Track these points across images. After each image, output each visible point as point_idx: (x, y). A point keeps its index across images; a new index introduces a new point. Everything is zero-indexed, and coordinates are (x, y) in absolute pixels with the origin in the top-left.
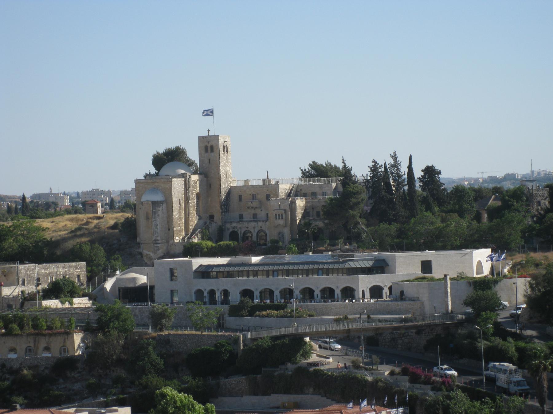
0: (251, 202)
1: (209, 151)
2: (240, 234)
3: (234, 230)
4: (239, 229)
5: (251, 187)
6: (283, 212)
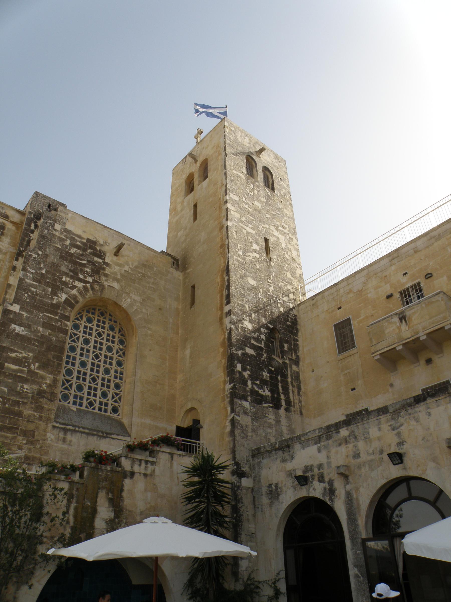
0: (396, 319)
1: (196, 183)
2: (352, 519)
3: (303, 493)
4: (338, 484)
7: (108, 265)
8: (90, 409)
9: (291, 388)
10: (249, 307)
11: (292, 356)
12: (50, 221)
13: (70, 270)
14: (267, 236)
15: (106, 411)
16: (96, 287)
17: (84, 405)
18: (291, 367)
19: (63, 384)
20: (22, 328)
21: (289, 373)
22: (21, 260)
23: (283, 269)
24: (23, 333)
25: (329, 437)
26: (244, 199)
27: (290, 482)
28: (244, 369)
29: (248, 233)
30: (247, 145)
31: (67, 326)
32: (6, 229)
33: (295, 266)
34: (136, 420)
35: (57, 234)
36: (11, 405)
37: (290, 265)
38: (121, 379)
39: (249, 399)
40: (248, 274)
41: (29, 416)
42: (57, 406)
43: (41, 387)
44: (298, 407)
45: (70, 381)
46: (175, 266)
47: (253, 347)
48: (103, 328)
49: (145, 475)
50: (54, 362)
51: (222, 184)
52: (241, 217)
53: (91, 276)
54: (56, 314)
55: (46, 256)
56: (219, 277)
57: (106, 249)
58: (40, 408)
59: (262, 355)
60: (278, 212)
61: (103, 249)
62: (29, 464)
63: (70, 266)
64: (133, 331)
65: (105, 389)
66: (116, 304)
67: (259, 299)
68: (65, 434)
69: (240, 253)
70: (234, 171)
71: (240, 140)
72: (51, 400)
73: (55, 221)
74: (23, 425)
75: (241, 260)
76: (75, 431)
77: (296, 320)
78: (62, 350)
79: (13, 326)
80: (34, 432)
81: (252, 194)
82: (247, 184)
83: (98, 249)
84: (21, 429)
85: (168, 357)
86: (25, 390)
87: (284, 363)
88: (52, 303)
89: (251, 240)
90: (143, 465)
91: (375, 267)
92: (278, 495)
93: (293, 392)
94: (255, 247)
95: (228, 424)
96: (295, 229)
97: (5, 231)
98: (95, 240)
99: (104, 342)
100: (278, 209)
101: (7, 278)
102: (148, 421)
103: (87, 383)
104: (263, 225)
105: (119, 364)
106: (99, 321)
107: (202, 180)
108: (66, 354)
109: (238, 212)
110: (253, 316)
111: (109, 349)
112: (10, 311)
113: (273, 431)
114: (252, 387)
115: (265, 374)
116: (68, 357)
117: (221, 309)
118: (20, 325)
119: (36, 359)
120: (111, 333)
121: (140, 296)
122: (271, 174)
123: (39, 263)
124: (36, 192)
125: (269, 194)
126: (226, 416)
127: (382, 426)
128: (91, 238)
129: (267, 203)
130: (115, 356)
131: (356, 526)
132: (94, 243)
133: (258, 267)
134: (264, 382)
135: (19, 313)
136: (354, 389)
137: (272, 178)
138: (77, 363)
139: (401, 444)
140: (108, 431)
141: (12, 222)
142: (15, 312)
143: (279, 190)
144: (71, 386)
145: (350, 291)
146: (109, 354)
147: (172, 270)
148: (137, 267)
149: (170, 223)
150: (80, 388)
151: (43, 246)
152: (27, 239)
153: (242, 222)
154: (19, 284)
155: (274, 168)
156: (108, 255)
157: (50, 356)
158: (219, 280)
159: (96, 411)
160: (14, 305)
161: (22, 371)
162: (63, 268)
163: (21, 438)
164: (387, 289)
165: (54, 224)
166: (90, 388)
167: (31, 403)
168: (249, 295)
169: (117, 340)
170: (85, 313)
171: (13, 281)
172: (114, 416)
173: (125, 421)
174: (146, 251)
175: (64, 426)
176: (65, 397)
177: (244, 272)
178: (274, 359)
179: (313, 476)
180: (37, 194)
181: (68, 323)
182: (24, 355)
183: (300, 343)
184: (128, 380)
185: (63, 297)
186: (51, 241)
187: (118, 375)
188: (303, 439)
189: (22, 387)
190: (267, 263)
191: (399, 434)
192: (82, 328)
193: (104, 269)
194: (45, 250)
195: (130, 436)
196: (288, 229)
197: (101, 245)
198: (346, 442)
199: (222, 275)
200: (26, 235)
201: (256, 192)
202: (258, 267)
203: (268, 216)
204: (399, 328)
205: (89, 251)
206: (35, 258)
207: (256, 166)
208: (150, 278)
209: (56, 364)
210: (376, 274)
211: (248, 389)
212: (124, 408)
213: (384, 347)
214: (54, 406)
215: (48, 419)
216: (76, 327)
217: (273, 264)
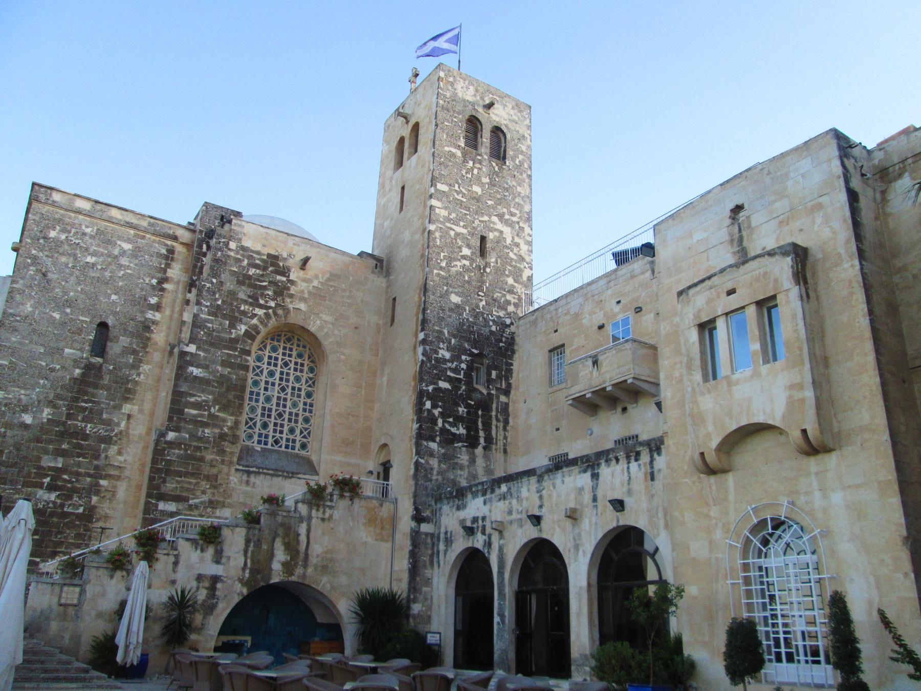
0: (590, 362)
5: (602, 283)
6: (784, 267)
7: (293, 282)
8: (276, 448)
9: (494, 422)
10: (448, 332)
11: (501, 385)
12: (223, 240)
13: (249, 297)
14: (485, 232)
15: (293, 448)
16: (280, 312)
17: (270, 444)
18: (498, 398)
19: (247, 423)
20: (200, 370)
21: (494, 406)
22: (194, 291)
23: (503, 274)
24: (201, 375)
25: (493, 491)
26: (456, 188)
27: (461, 531)
28: (434, 406)
29: (457, 234)
30: (470, 99)
31: (247, 361)
32: (176, 253)
33: (522, 266)
34: (325, 457)
35: (232, 254)
36: (193, 451)
37: (515, 267)
38: (311, 412)
39: (438, 439)
40: (451, 289)
41: (212, 461)
42: (239, 447)
43: (222, 429)
44: (502, 444)
45: (254, 419)
46: (378, 269)
47: (449, 380)
48: (290, 356)
49: (323, 520)
50: (235, 402)
51: (429, 168)
52: (450, 214)
53: (273, 300)
54: (235, 349)
55: (222, 283)
56: (417, 296)
57: (291, 262)
58: (221, 452)
59: (460, 388)
60: (507, 194)
61: (286, 264)
62: (213, 508)
63: (249, 291)
64: (323, 357)
65: (293, 424)
66: (303, 328)
67: (463, 320)
68: (248, 476)
69: (443, 264)
70: (447, 149)
71: (460, 95)
72: (233, 443)
73: (231, 238)
74: (206, 470)
75: (442, 273)
76: (259, 473)
77: (513, 339)
78: (243, 389)
79: (191, 369)
80: (217, 476)
81: (469, 176)
82: (464, 162)
83: (281, 264)
84: (204, 475)
85: (364, 384)
86: (206, 435)
87: (489, 394)
88: (230, 338)
89: (460, 243)
90: (321, 510)
91: (593, 287)
92: (452, 542)
93: (497, 427)
94: (466, 251)
95: (412, 467)
96: (530, 213)
97: (175, 256)
98: (277, 254)
99: (292, 371)
100: (507, 190)
101: (181, 315)
102: (339, 458)
103: (273, 420)
104: (481, 219)
105: (309, 395)
106: (285, 348)
107: (413, 151)
108: (248, 390)
109: (446, 208)
110: (453, 341)
111: (298, 379)
112: (186, 352)
113: (465, 473)
114: (443, 425)
115: (462, 410)
116: (252, 393)
117: (416, 336)
118: (198, 367)
119: (216, 401)
120: (299, 361)
121: (331, 315)
122: (504, 135)
123: (214, 294)
124: (206, 203)
125: (496, 169)
126: (412, 458)
127: (530, 487)
128: (273, 252)
129: (492, 184)
130: (304, 387)
131: (503, 579)
132: (276, 258)
133: (466, 278)
134: (459, 419)
135: (196, 354)
136: (558, 429)
137: (505, 143)
138: (262, 398)
139: (541, 507)
140: (295, 471)
141: (182, 243)
142: (192, 354)
143: (513, 159)
144: (255, 424)
145: (568, 313)
146: (297, 385)
147: (372, 277)
148: (329, 280)
149: (378, 204)
150: (265, 426)
151: (217, 273)
152: (199, 264)
153: (449, 220)
154: (194, 322)
155: (510, 126)
156: (293, 270)
157: (231, 397)
158: (416, 299)
159: (283, 449)
160: (190, 345)
161: (202, 416)
162: (242, 296)
163: (204, 483)
164: (599, 318)
165: (228, 243)
166: (275, 424)
167: (213, 447)
168: (450, 317)
169: (306, 368)
170: (269, 341)
171: (187, 317)
172: (303, 453)
173: (314, 458)
174: (339, 257)
175: (247, 469)
176: (250, 437)
177: (445, 288)
178: (478, 390)
179: (478, 527)
180: (206, 204)
181: (249, 358)
182: (203, 398)
183: (515, 368)
184: (317, 413)
185: (243, 328)
186: (225, 263)
187: (308, 407)
188: (474, 489)
189: (203, 431)
190: (480, 270)
191: (541, 497)
192: (266, 359)
193: (288, 289)
194: (219, 276)
195: (318, 474)
196: (518, 215)
197: (285, 259)
198: (505, 498)
199: (419, 294)
200: (198, 260)
201: (475, 171)
202: (466, 278)
203: (490, 203)
204: (591, 373)
205: (271, 269)
206: (209, 288)
207: (482, 130)
208: (344, 290)
209: (237, 404)
210: (593, 296)
211: (437, 428)
212: (313, 444)
213: (577, 390)
214: (236, 449)
215: (231, 463)
216: (259, 359)
217: (488, 270)
